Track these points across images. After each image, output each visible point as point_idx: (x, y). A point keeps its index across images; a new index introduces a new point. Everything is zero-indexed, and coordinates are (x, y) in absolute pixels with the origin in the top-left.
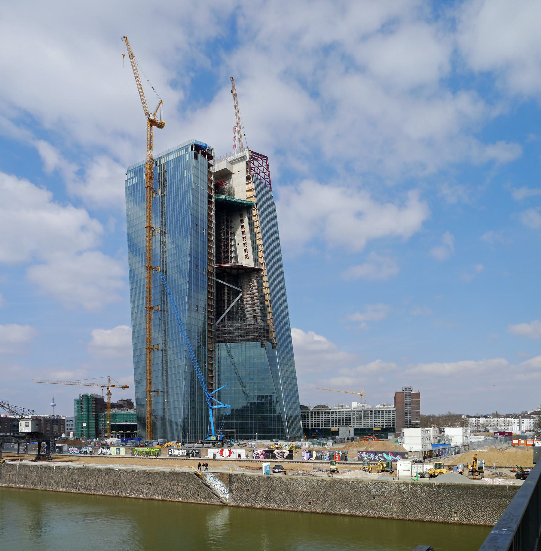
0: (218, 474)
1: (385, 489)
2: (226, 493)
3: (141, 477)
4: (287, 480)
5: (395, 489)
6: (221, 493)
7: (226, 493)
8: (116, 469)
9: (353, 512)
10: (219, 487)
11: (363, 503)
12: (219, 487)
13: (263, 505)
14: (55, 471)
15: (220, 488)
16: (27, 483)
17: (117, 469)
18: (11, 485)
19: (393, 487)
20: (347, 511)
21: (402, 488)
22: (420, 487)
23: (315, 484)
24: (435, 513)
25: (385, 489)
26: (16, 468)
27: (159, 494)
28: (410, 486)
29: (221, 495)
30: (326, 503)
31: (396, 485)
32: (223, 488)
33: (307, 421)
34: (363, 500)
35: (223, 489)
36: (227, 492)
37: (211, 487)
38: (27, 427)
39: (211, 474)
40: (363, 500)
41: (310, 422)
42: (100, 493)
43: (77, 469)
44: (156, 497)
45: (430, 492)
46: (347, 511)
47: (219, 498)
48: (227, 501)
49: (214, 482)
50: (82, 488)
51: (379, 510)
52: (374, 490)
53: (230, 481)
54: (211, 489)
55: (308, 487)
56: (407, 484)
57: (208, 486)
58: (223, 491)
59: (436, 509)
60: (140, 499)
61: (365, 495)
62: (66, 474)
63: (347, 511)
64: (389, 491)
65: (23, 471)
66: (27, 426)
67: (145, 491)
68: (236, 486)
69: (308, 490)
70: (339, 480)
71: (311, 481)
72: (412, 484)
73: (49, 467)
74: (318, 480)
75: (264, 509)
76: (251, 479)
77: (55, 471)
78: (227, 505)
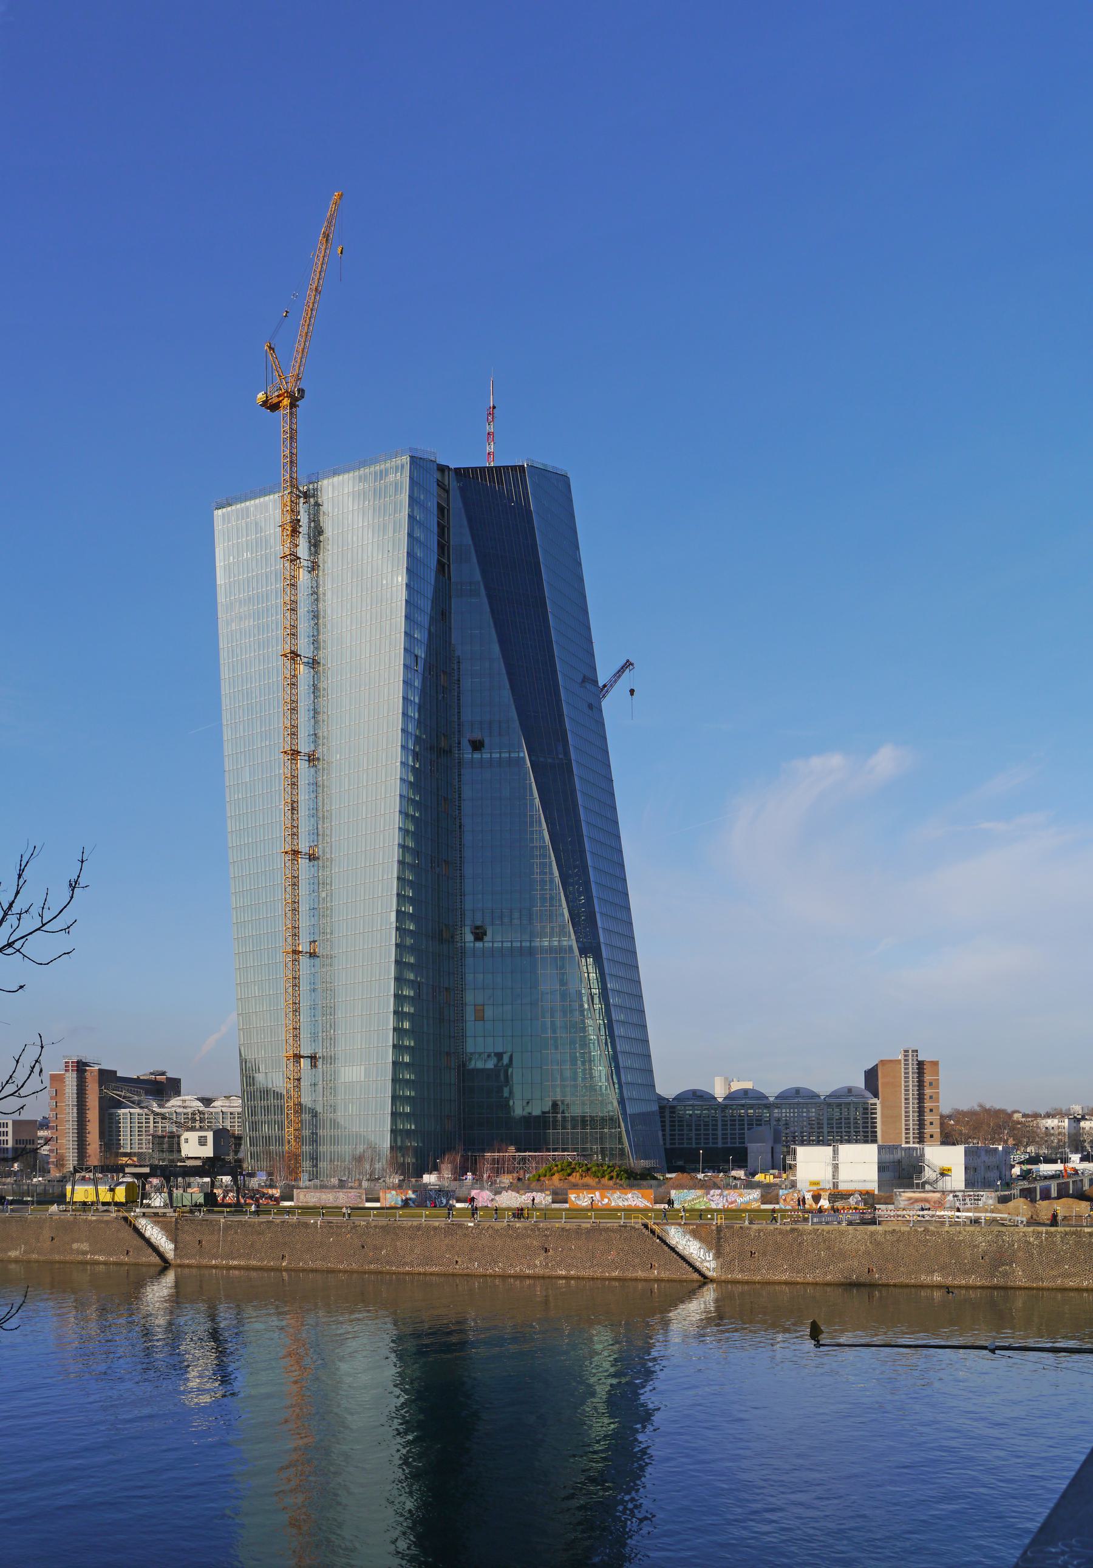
0: (691, 1227)
1: (1003, 1242)
2: (708, 1259)
3: (529, 1236)
4: (828, 1232)
5: (1019, 1240)
6: (699, 1259)
7: (708, 1259)
8: (470, 1224)
9: (950, 1281)
10: (693, 1248)
11: (965, 1264)
12: (693, 1248)
13: (784, 1277)
14: (320, 1231)
15: (695, 1252)
16: (248, 1256)
17: (472, 1224)
18: (205, 1262)
19: (1016, 1238)
20: (937, 1278)
21: (1031, 1239)
22: (1061, 1237)
23: (879, 1238)
24: (1085, 1275)
25: (1003, 1242)
26: (216, 1228)
27: (569, 1267)
28: (1044, 1235)
29: (698, 1264)
30: (902, 1269)
31: (1021, 1234)
32: (702, 1250)
33: (713, 1130)
34: (966, 1261)
35: (702, 1253)
36: (711, 1258)
37: (676, 1249)
38: (202, 1145)
39: (677, 1227)
40: (966, 1261)
41: (720, 1132)
42: (435, 1269)
43: (376, 1227)
44: (563, 1273)
45: (1077, 1243)
46: (939, 1279)
47: (697, 1270)
48: (710, 1274)
49: (684, 1242)
50: (388, 1263)
51: (993, 1276)
52: (984, 1244)
53: (719, 1239)
54: (677, 1253)
55: (868, 1244)
56: (1038, 1233)
57: (673, 1249)
58: (701, 1256)
59: (1086, 1269)
60: (529, 1277)
61: (968, 1254)
62: (349, 1236)
63: (939, 1279)
64: (1009, 1244)
65: (236, 1233)
66: (202, 1142)
67: (537, 1262)
68: (727, 1249)
69: (868, 1247)
70: (922, 1229)
71: (872, 1233)
72: (1046, 1233)
73: (306, 1225)
74: (886, 1231)
75: (786, 1283)
76: (759, 1233)
77: (320, 1231)
78: (712, 1281)
